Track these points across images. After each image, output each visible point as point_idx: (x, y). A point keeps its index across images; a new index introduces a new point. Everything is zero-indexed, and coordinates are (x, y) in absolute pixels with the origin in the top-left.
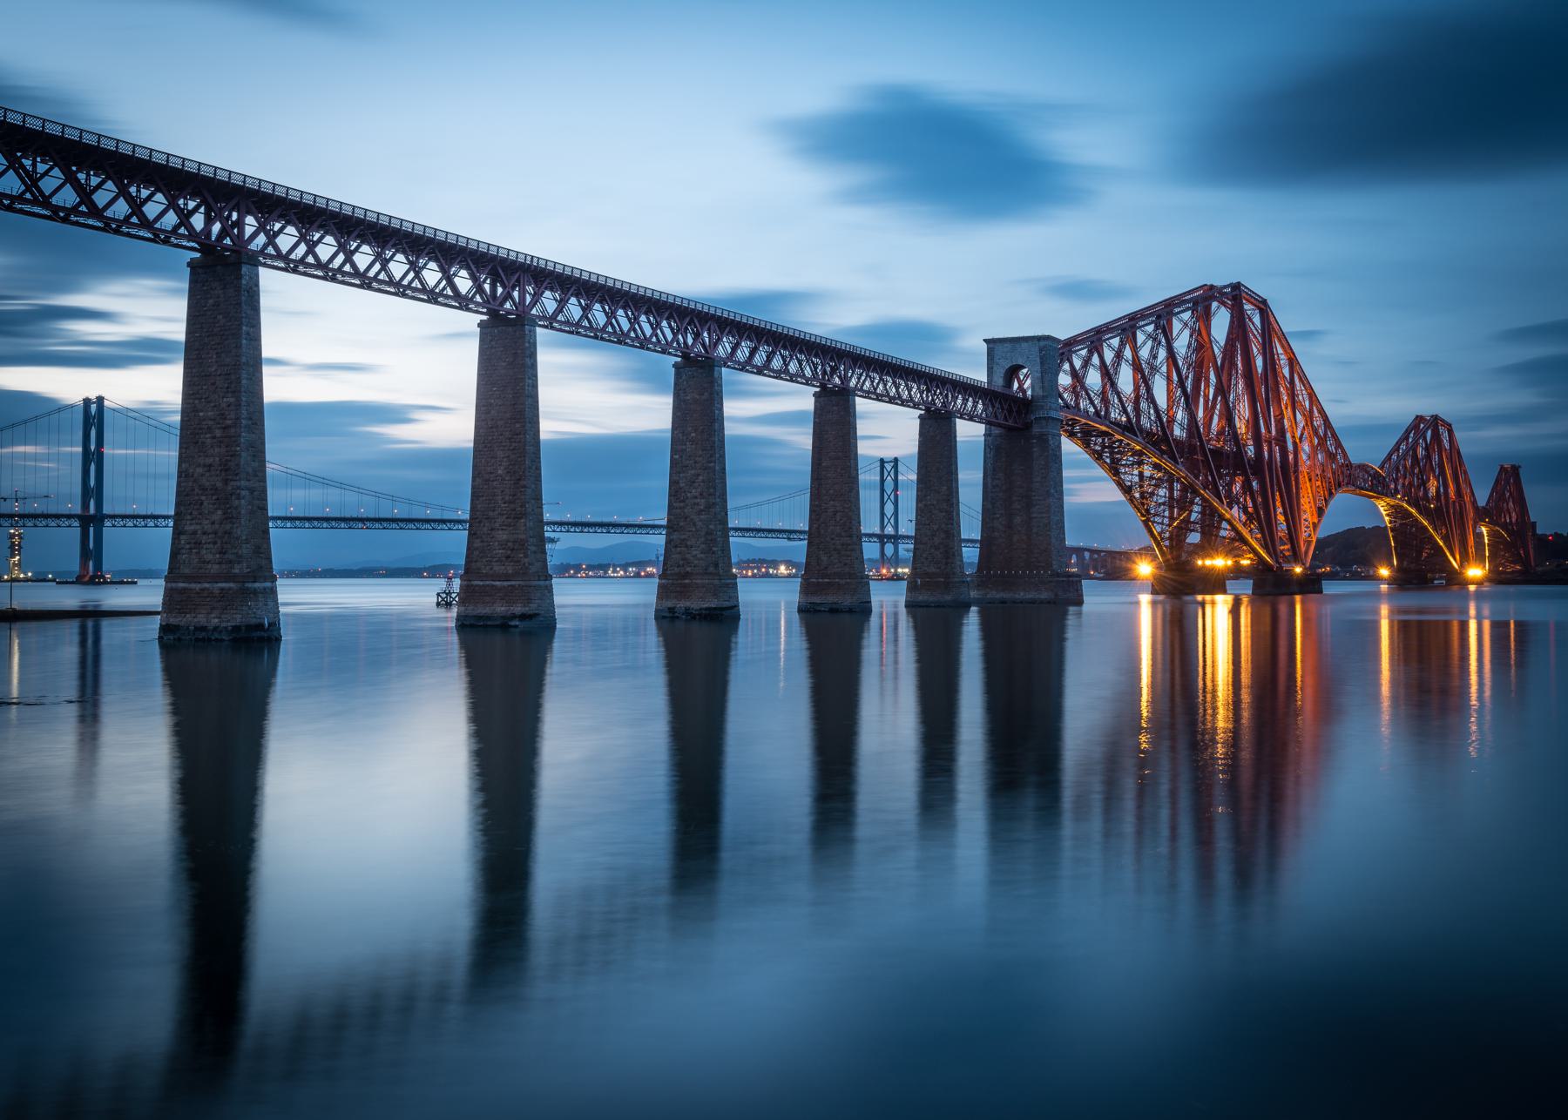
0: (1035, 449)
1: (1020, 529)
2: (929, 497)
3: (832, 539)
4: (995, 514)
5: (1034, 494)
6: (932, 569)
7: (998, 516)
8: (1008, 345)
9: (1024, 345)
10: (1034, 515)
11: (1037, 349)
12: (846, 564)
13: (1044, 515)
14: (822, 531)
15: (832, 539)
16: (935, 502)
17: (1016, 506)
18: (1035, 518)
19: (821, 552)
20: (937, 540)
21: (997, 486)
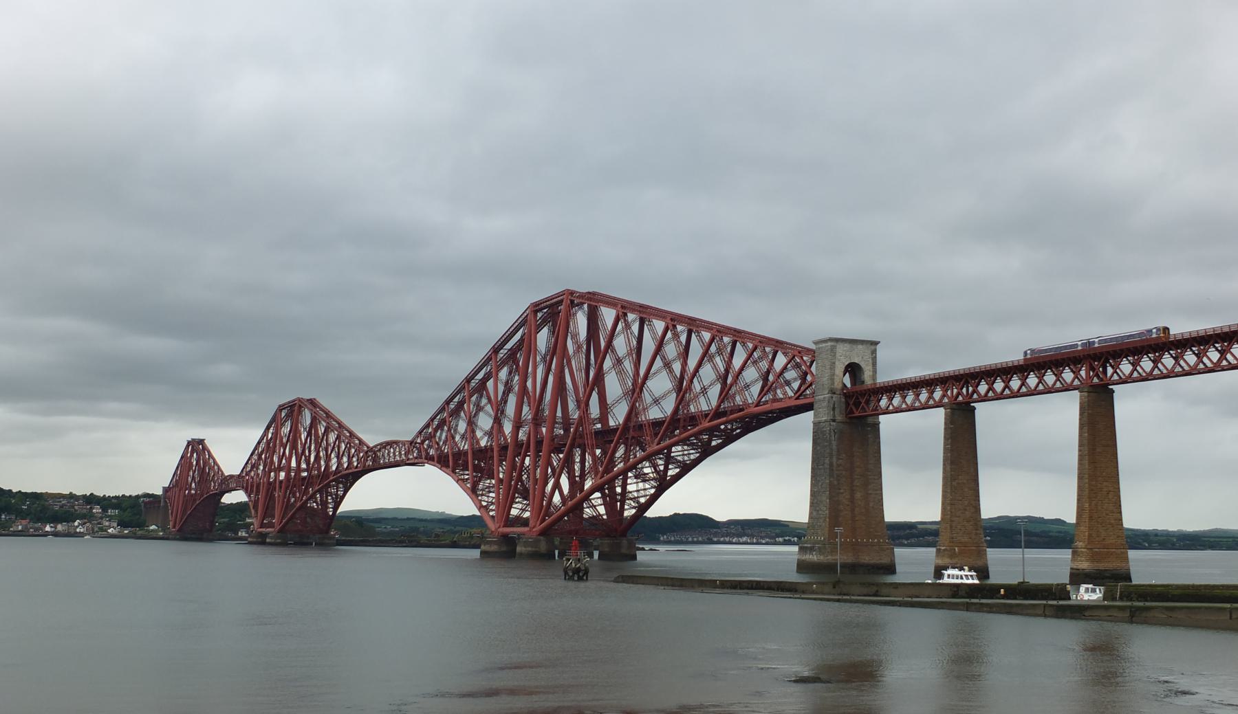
0: (870, 436)
1: (860, 503)
2: (960, 477)
3: (1107, 514)
4: (840, 489)
5: (869, 473)
6: (965, 539)
7: (842, 491)
8: (847, 347)
9: (860, 347)
10: (870, 492)
11: (869, 352)
12: (1118, 537)
13: (878, 492)
14: (1099, 508)
15: (1107, 514)
16: (965, 481)
17: (857, 483)
18: (871, 494)
19: (1099, 526)
20: (968, 514)
21: (841, 465)
